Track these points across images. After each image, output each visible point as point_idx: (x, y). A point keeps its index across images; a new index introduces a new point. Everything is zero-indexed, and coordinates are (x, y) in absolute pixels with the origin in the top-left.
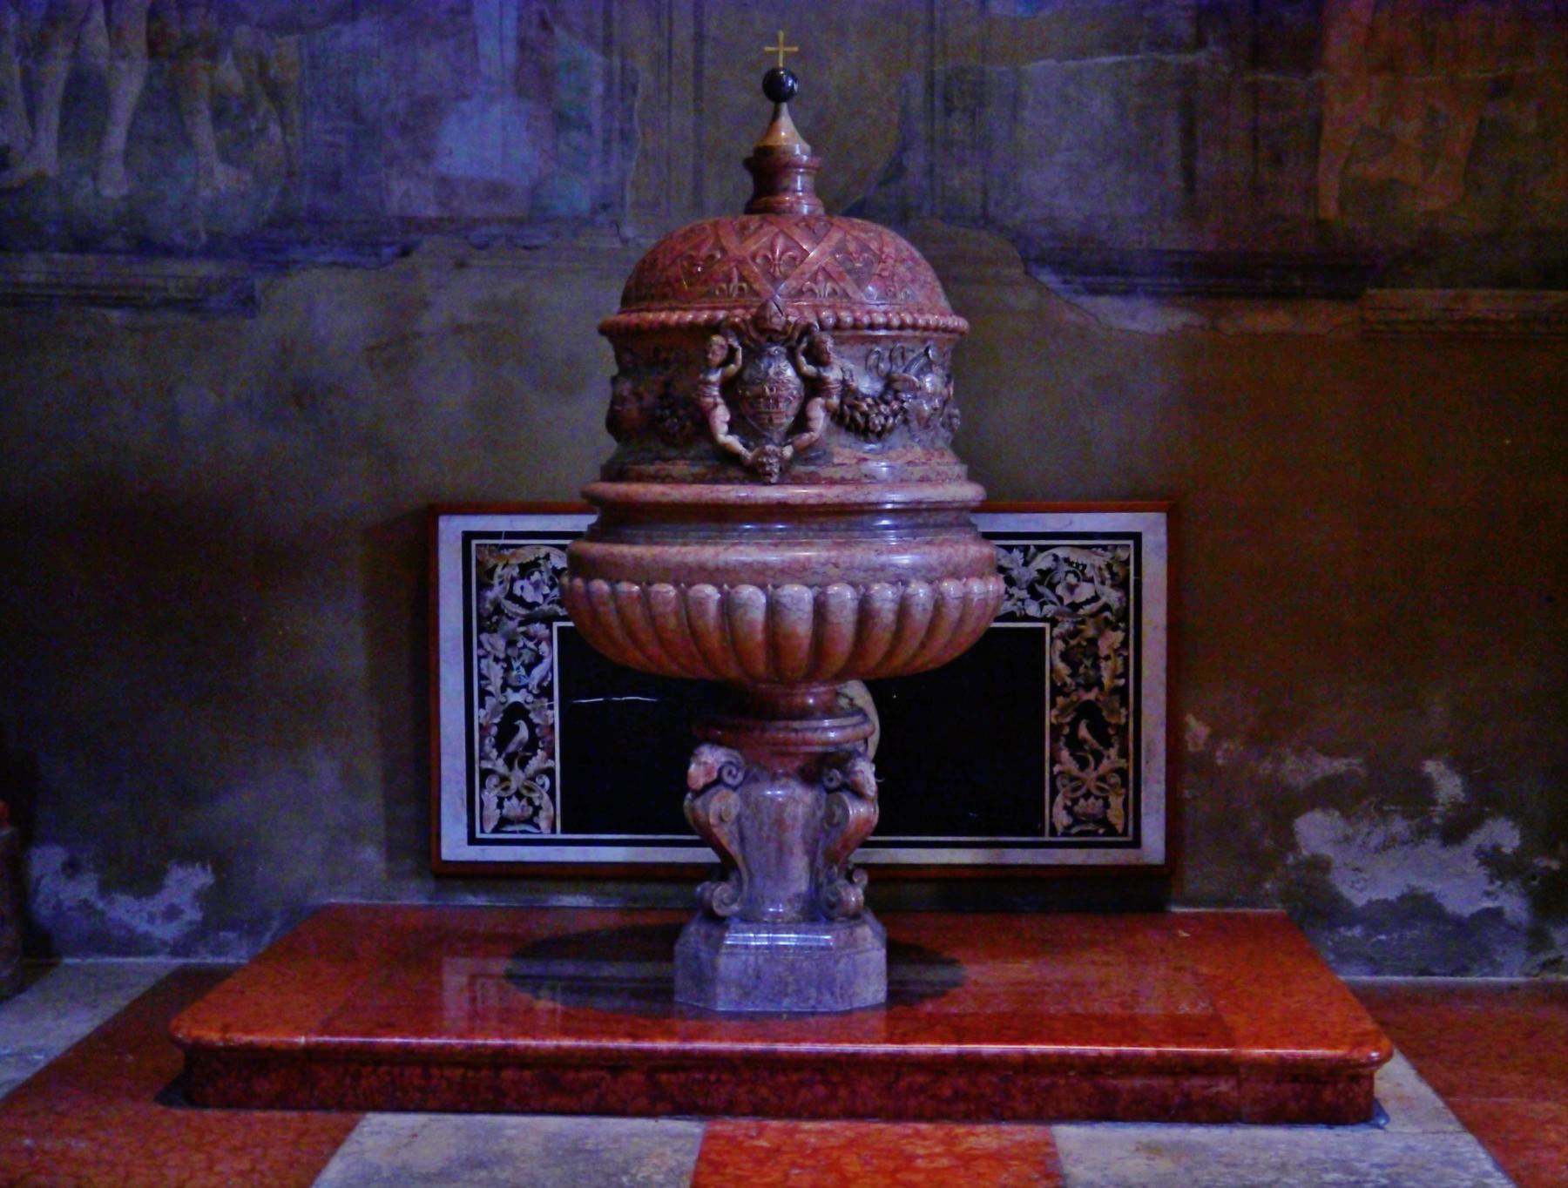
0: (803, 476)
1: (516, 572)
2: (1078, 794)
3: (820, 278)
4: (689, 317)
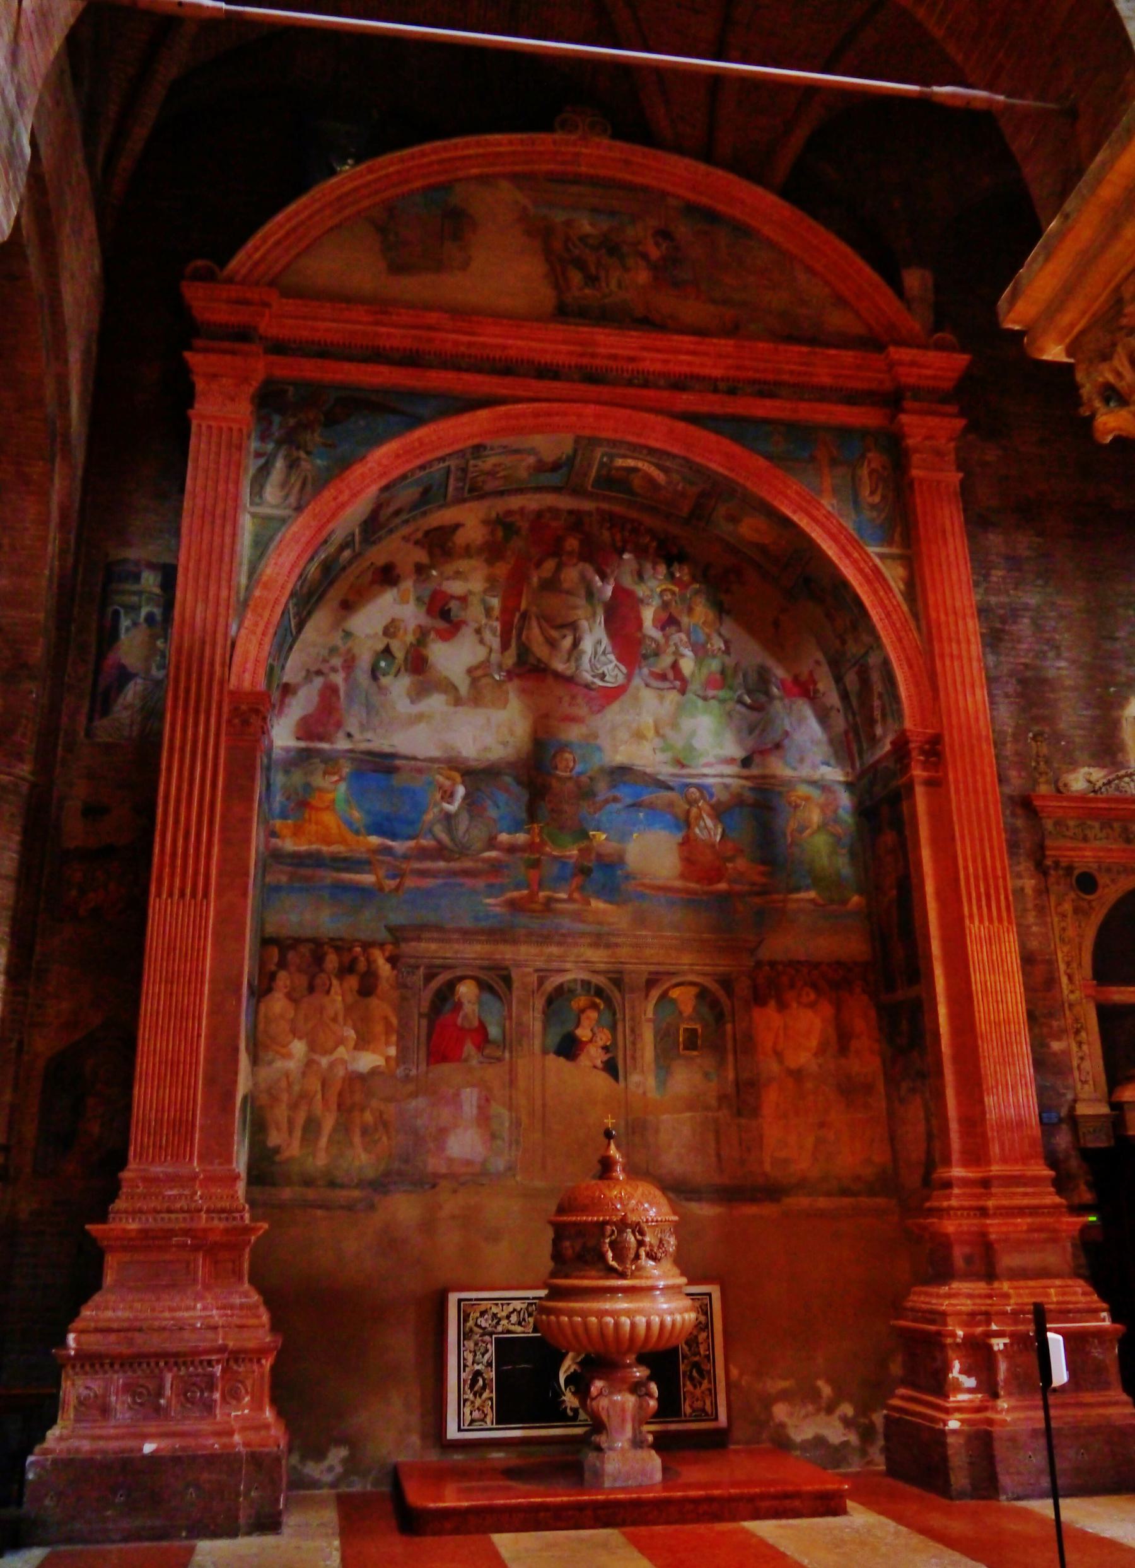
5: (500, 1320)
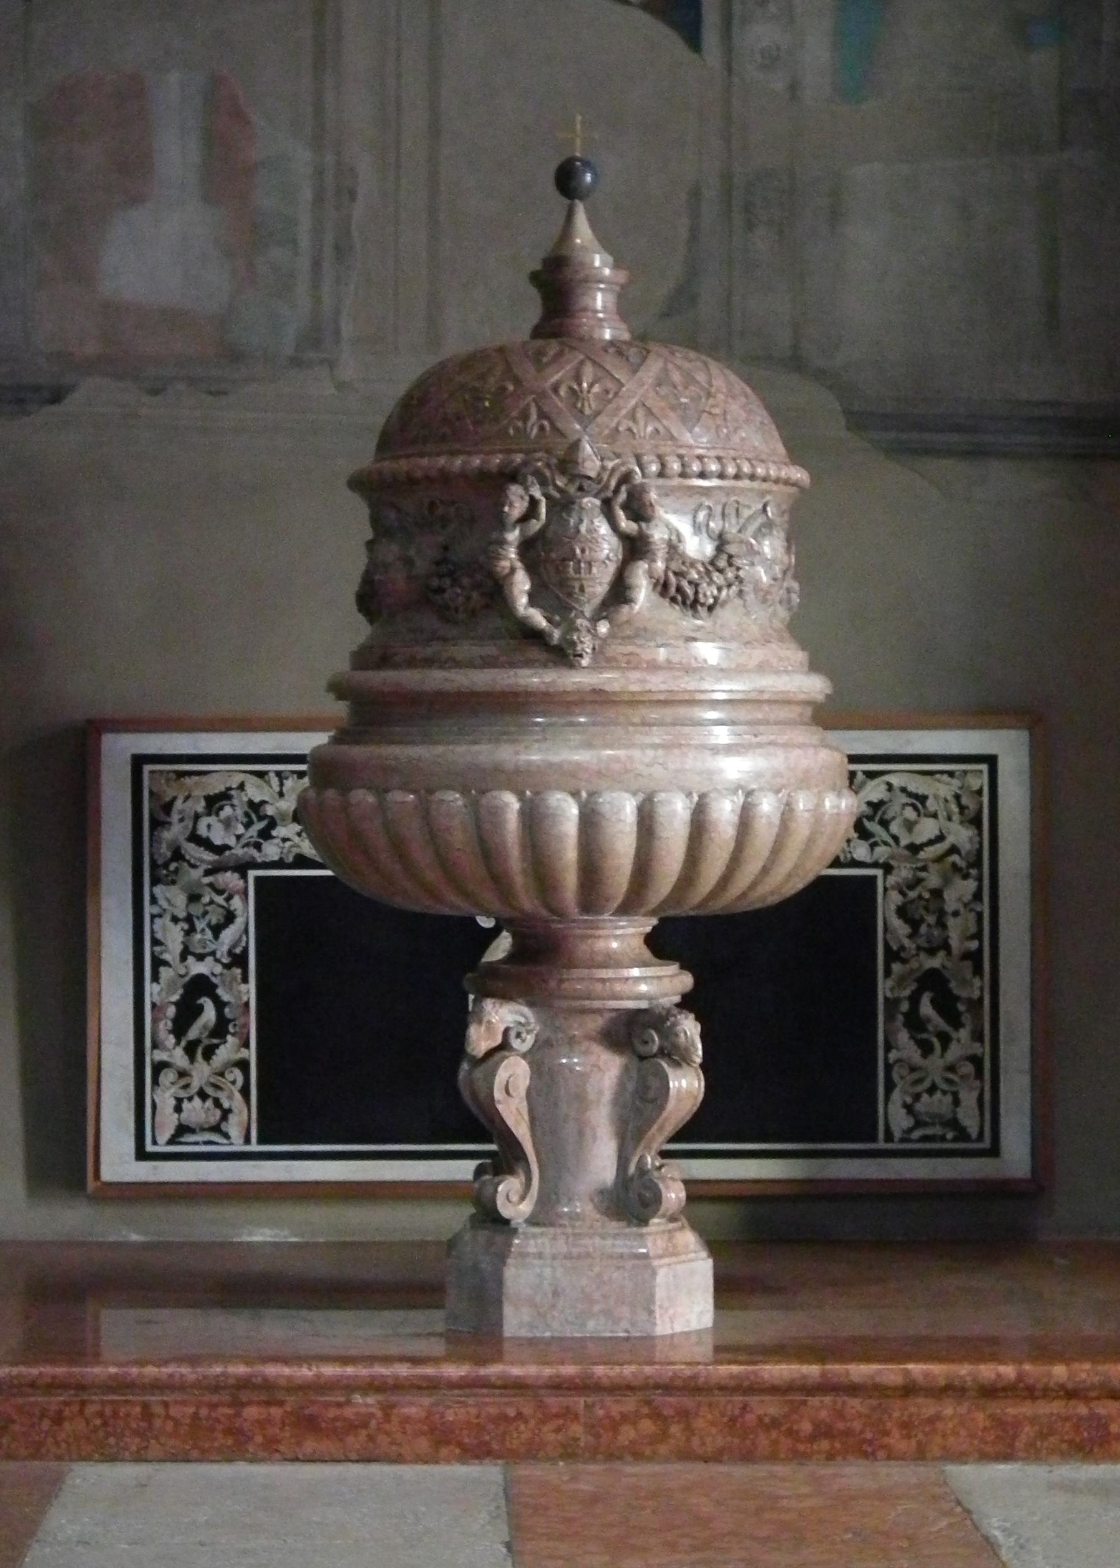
0: (620, 658)
1: (201, 806)
2: (919, 1088)
3: (640, 414)
4: (477, 462)
5: (272, 823)
